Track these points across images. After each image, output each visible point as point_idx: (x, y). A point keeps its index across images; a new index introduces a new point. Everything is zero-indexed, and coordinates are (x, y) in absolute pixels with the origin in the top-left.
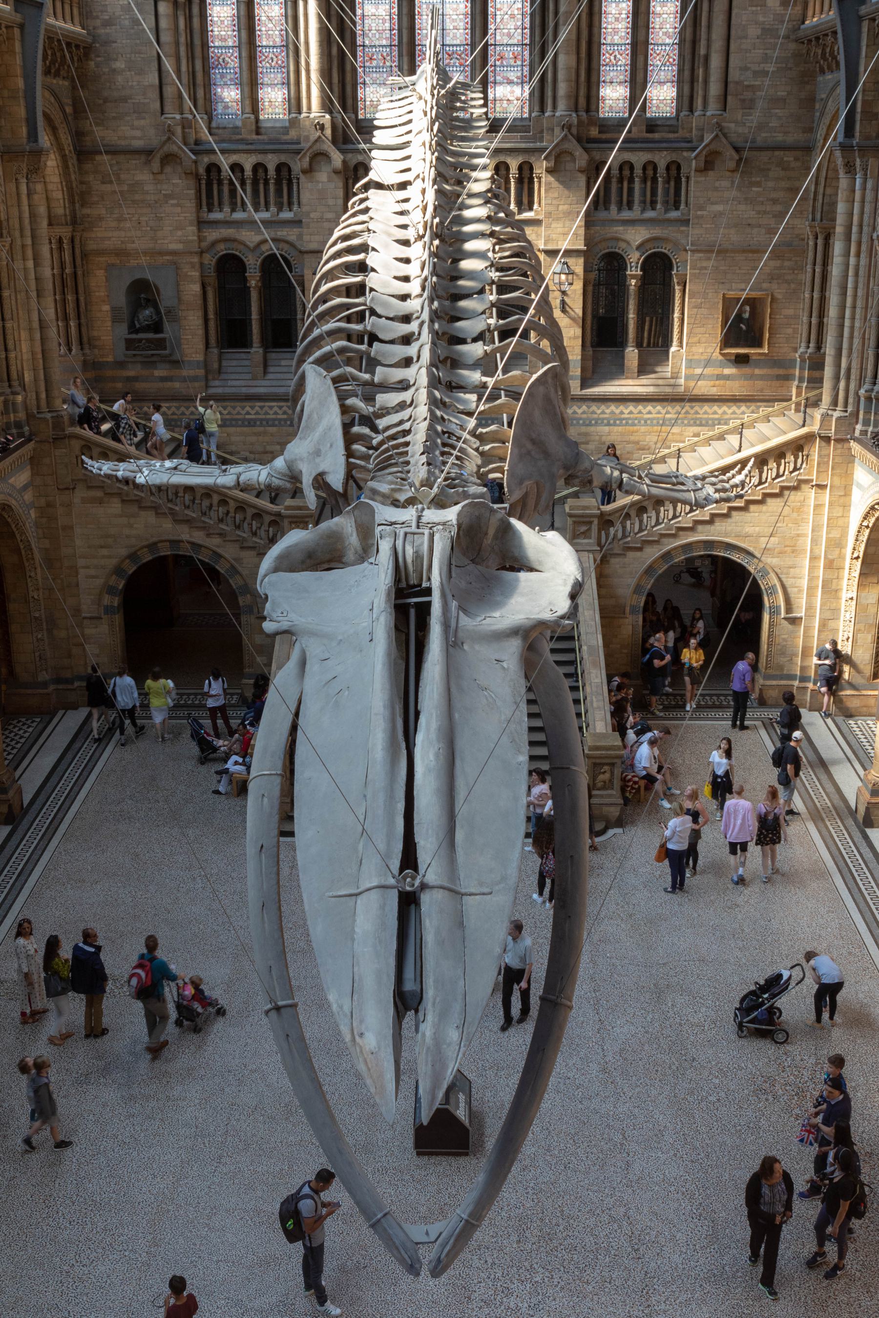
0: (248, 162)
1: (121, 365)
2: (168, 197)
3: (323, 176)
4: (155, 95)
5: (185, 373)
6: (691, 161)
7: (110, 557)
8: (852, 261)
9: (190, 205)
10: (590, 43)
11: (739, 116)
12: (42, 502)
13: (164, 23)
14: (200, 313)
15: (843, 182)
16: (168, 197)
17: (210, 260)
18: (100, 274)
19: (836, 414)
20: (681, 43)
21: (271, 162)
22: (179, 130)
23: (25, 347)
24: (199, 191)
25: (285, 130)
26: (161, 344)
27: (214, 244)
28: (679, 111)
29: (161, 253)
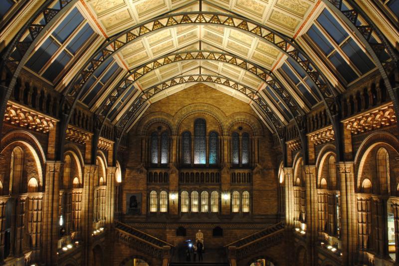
2: (141, 179)
3: (174, 175)
8: (290, 192)
9: (146, 180)
13: (144, 145)
16: (141, 179)
23: (106, 209)
24: (147, 178)
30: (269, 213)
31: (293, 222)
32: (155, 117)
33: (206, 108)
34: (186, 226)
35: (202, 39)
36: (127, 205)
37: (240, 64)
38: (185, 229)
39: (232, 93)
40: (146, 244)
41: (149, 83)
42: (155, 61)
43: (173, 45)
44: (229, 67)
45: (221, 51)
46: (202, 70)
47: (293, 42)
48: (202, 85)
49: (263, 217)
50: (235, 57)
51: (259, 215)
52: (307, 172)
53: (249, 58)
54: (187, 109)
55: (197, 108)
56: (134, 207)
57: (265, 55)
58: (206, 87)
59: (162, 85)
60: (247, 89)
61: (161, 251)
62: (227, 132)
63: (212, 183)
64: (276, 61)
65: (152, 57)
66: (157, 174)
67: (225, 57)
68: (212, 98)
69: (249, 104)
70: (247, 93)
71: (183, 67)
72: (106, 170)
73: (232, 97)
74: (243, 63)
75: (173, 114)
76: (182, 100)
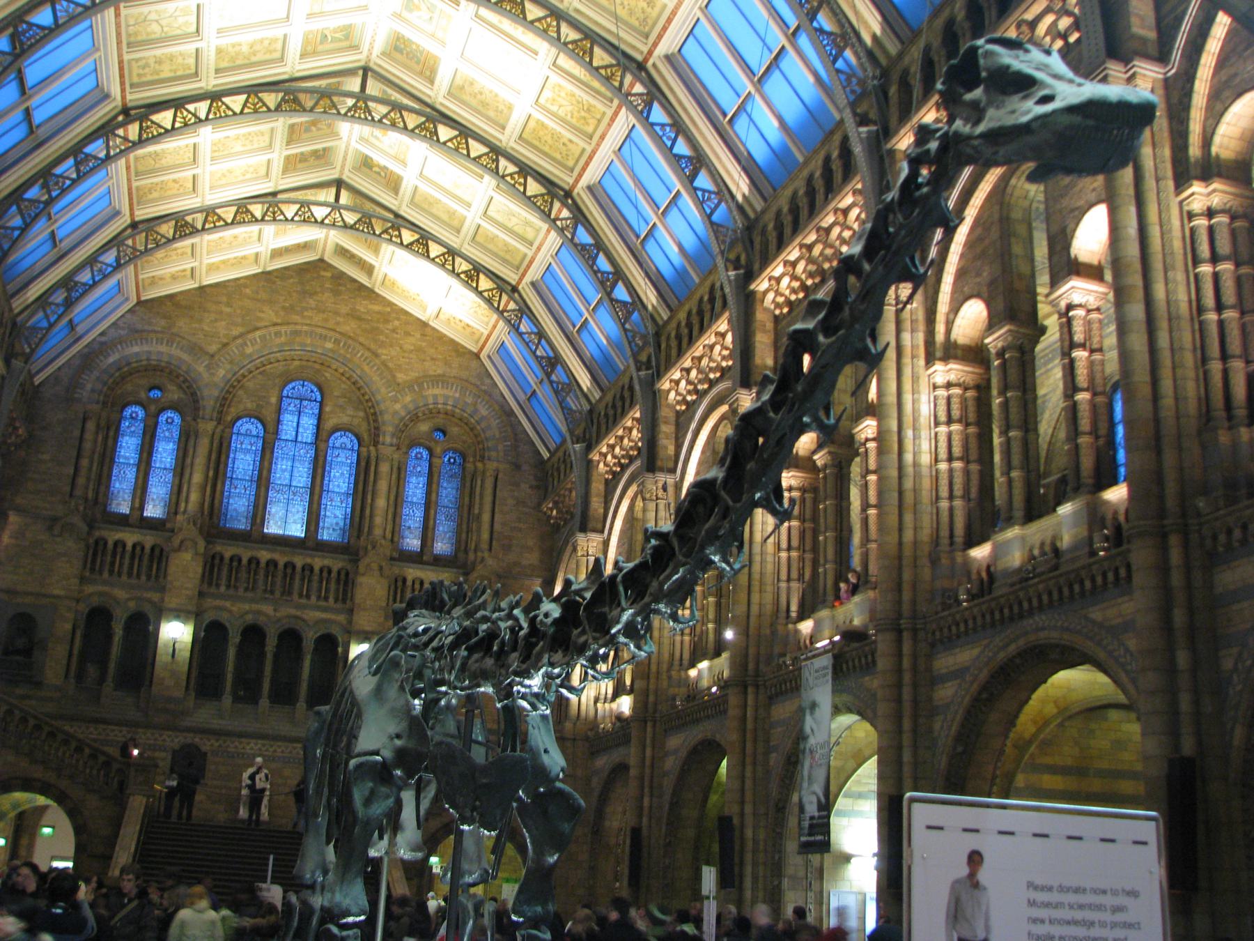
3: (187, 556)
13: (89, 436)
14: (68, 647)
17: (83, 608)
22: (81, 508)
24: (86, 556)
27: (91, 595)
28: (457, 550)
29: (45, 596)
31: (592, 712)
32: (146, 348)
33: (329, 345)
34: (207, 744)
35: (377, 61)
38: (205, 754)
42: (215, 96)
43: (282, 59)
48: (325, 270)
50: (465, 132)
52: (648, 496)
53: (507, 139)
55: (298, 339)
57: (559, 129)
58: (340, 276)
60: (482, 276)
62: (393, 435)
63: (322, 603)
64: (589, 149)
65: (210, 82)
66: (124, 546)
67: (435, 127)
68: (354, 315)
69: (477, 356)
73: (425, 325)
75: (213, 348)
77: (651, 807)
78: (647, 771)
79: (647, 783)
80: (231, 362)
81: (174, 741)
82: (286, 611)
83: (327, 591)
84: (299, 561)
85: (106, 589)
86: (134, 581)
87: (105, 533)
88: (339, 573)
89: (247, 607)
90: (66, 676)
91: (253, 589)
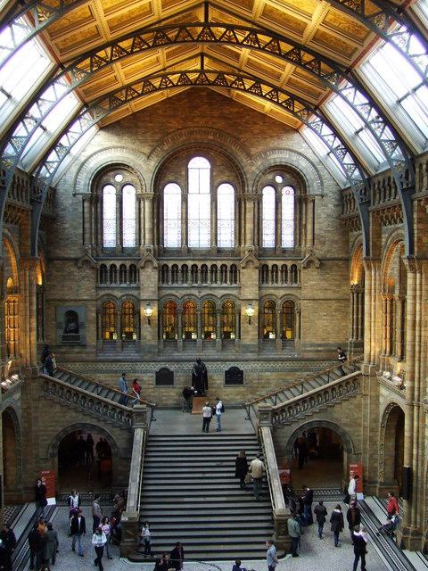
0: (118, 264)
1: (60, 347)
3: (149, 270)
4: (81, 237)
5: (86, 350)
6: (300, 264)
7: (53, 431)
8: (373, 303)
9: (93, 281)
10: (259, 220)
11: (319, 247)
12: (25, 406)
13: (86, 210)
15: (367, 273)
17: (99, 302)
18: (53, 308)
19: (371, 366)
20: (295, 219)
21: (128, 264)
23: (22, 339)
25: (134, 250)
26: (78, 338)
28: (295, 244)
30: (331, 341)
33: (211, 137)
34: (172, 367)
36: (58, 326)
37: (288, 54)
38: (172, 372)
39: (264, 106)
40: (100, 402)
41: (100, 87)
42: (113, 44)
43: (151, 11)
44: (265, 58)
45: (249, 25)
46: (206, 60)
47: (401, 14)
48: (203, 91)
49: (320, 349)
50: (277, 37)
51: (312, 345)
54: (173, 139)
55: (193, 136)
56: (71, 331)
59: (124, 92)
60: (296, 102)
61: (130, 414)
63: (224, 285)
64: (361, 49)
70: (296, 110)
71: (169, 56)
72: (19, 263)
73: (264, 116)
74: (293, 50)
76: (164, 120)
77: (417, 455)
78: (415, 435)
79: (415, 441)
80: (157, 156)
81: (158, 367)
82: (204, 292)
83: (226, 277)
84: (209, 264)
85: (110, 292)
86: (124, 285)
87: (104, 262)
88: (231, 267)
89: (184, 292)
90: (98, 338)
91: (187, 280)
